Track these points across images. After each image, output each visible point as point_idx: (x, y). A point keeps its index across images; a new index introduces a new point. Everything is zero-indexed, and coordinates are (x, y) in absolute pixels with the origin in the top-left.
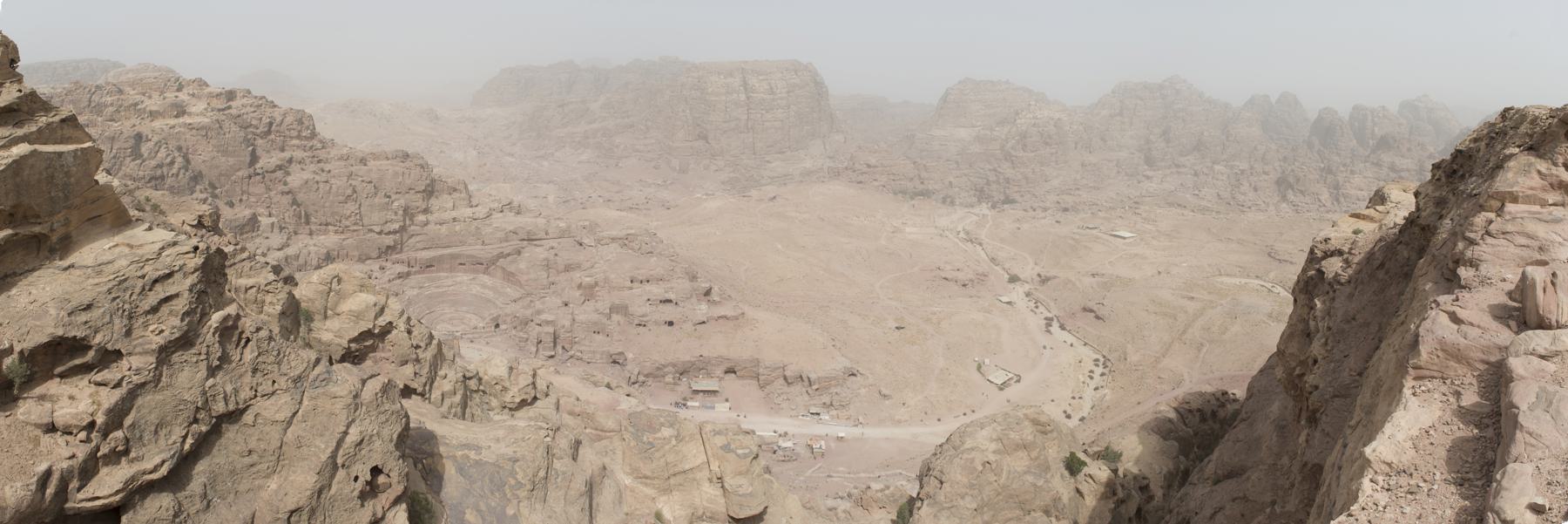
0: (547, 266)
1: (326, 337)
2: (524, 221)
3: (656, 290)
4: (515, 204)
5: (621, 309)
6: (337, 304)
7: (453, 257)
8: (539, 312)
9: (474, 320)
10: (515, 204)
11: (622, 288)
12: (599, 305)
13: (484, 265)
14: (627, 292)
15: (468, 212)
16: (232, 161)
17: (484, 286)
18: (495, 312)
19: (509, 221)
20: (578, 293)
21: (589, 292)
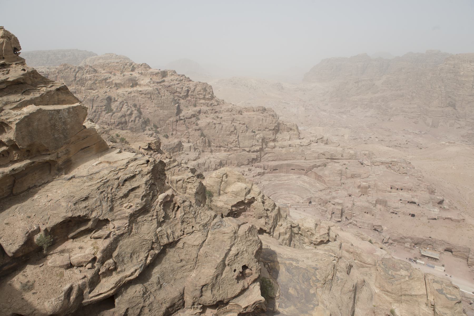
0: (341, 174)
1: (220, 204)
2: (330, 149)
4: (325, 139)
5: (384, 203)
6: (225, 188)
7: (288, 165)
8: (334, 198)
9: (298, 199)
10: (325, 139)
11: (385, 191)
12: (370, 198)
13: (306, 171)
15: (298, 141)
16: (166, 112)
17: (304, 182)
18: (309, 195)
19: (321, 148)
20: (357, 190)
21: (364, 190)
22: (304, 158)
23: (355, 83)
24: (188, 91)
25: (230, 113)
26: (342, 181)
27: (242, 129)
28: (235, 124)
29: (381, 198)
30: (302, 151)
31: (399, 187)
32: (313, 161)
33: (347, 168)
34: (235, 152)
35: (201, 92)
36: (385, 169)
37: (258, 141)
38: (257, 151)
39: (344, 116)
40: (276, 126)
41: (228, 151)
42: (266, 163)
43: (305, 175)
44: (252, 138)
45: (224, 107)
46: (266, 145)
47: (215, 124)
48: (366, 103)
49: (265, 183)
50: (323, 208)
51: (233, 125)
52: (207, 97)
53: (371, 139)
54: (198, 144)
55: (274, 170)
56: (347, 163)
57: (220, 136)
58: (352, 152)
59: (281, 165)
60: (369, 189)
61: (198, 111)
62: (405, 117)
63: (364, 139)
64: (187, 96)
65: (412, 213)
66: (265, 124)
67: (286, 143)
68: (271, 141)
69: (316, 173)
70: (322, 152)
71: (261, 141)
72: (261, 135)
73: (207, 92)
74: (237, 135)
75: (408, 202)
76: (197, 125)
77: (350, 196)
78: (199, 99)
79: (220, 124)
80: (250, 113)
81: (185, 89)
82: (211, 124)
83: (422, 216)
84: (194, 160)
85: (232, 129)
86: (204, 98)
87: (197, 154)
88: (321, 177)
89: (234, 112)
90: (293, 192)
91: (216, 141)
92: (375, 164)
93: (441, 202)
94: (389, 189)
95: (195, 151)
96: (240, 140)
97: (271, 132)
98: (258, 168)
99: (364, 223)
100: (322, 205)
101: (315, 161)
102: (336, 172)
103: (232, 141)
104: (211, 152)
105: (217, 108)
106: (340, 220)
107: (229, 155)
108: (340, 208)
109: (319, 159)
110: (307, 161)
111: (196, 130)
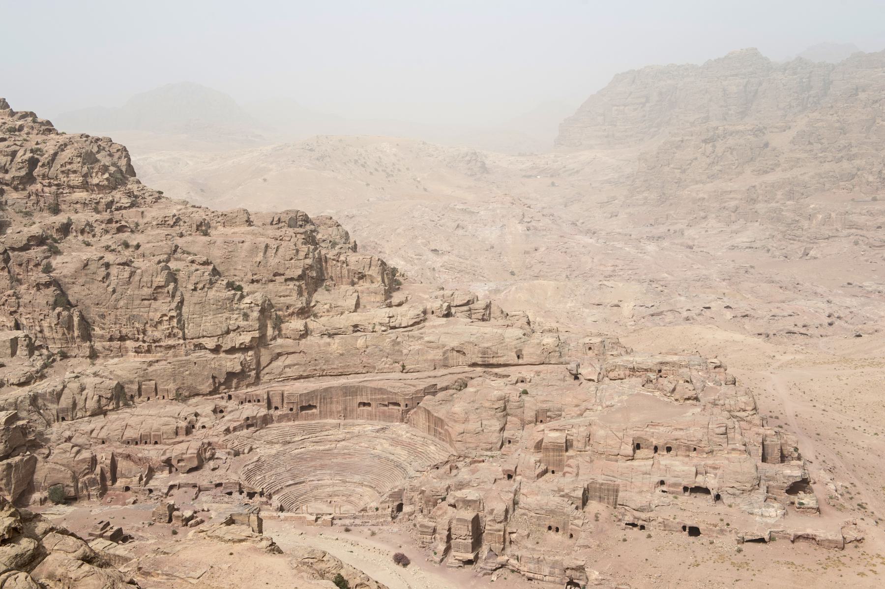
0: (504, 409)
2: (487, 332)
3: (680, 468)
5: (610, 494)
7: (349, 391)
8: (461, 486)
9: (370, 500)
10: (480, 304)
12: (569, 478)
13: (404, 407)
14: (623, 464)
15: (381, 314)
17: (396, 442)
18: (400, 483)
22: (398, 366)
23: (705, 141)
24: (33, 163)
25: (169, 231)
26: (506, 434)
27: (194, 279)
28: (173, 265)
29: (600, 479)
30: (395, 343)
31: (660, 442)
32: (426, 374)
33: (525, 392)
34: (171, 352)
35: (75, 166)
36: (639, 389)
37: (246, 316)
38: (244, 349)
39: (651, 247)
40: (311, 267)
41: (149, 351)
42: (277, 388)
43: (402, 420)
44: (226, 306)
45: (154, 213)
46: (277, 326)
47: (107, 265)
48: (733, 204)
49: (264, 451)
50: (426, 522)
51: (167, 268)
52: (95, 181)
54: (47, 333)
55: (303, 408)
57: (121, 303)
58: (549, 340)
59: (326, 390)
60: (571, 453)
61: (57, 226)
62: (856, 243)
63: (685, 314)
64: (29, 179)
65: (689, 523)
66: (273, 261)
67: (345, 321)
68: (292, 314)
69: (428, 412)
70: (455, 343)
71: (255, 314)
72: (259, 297)
73: (109, 171)
74: (177, 299)
75: (686, 489)
76: (48, 269)
77: (510, 477)
78: (69, 186)
79: (124, 264)
80: (236, 230)
81: (23, 156)
82: (92, 267)
83: (722, 531)
84: (21, 385)
85: (160, 279)
86: (85, 186)
87: (39, 364)
88: (439, 422)
89: (183, 228)
90: (357, 478)
91: (106, 321)
92: (612, 375)
93: (799, 486)
94: (629, 450)
95: (31, 354)
96: (185, 316)
97: (291, 285)
98: (247, 405)
99: (538, 561)
100: (425, 511)
101: (432, 373)
102: (487, 404)
103: (157, 316)
104: (93, 355)
105: (130, 216)
106: (471, 556)
107: (151, 364)
108: (469, 515)
109: (446, 366)
110: (409, 376)
111: (38, 286)
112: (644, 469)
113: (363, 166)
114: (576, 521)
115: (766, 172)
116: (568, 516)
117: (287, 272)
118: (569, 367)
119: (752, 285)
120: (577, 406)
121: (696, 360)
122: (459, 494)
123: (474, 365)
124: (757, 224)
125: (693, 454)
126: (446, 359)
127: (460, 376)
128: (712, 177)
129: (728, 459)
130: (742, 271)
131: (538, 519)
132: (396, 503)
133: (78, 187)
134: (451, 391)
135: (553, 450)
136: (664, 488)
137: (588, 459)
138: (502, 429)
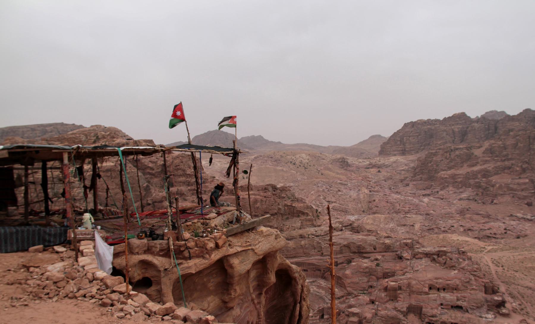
0: (369, 273)
3: (449, 297)
8: (351, 306)
11: (420, 293)
17: (319, 287)
20: (383, 295)
21: (393, 294)
26: (370, 284)
29: (414, 303)
31: (441, 286)
39: (426, 200)
48: (460, 180)
53: (453, 229)
56: (379, 257)
63: (443, 229)
67: (295, 233)
70: (345, 243)
75: (452, 307)
78: (178, 175)
88: (339, 278)
94: (427, 289)
102: (361, 270)
108: (355, 319)
110: (325, 258)
112: (434, 298)
113: (294, 164)
114: (403, 322)
115: (473, 166)
116: (400, 319)
117: (270, 211)
118: (397, 253)
119: (469, 216)
120: (401, 270)
121: (454, 249)
122: (350, 310)
123: (354, 253)
124: (470, 189)
125: (455, 291)
126: (342, 250)
127: (348, 258)
128: (450, 168)
129: (470, 293)
130: (465, 210)
131: (386, 321)
132: (321, 314)
133: (181, 175)
134: (344, 264)
135: (393, 290)
136: (442, 307)
137: (408, 294)
138: (368, 281)
